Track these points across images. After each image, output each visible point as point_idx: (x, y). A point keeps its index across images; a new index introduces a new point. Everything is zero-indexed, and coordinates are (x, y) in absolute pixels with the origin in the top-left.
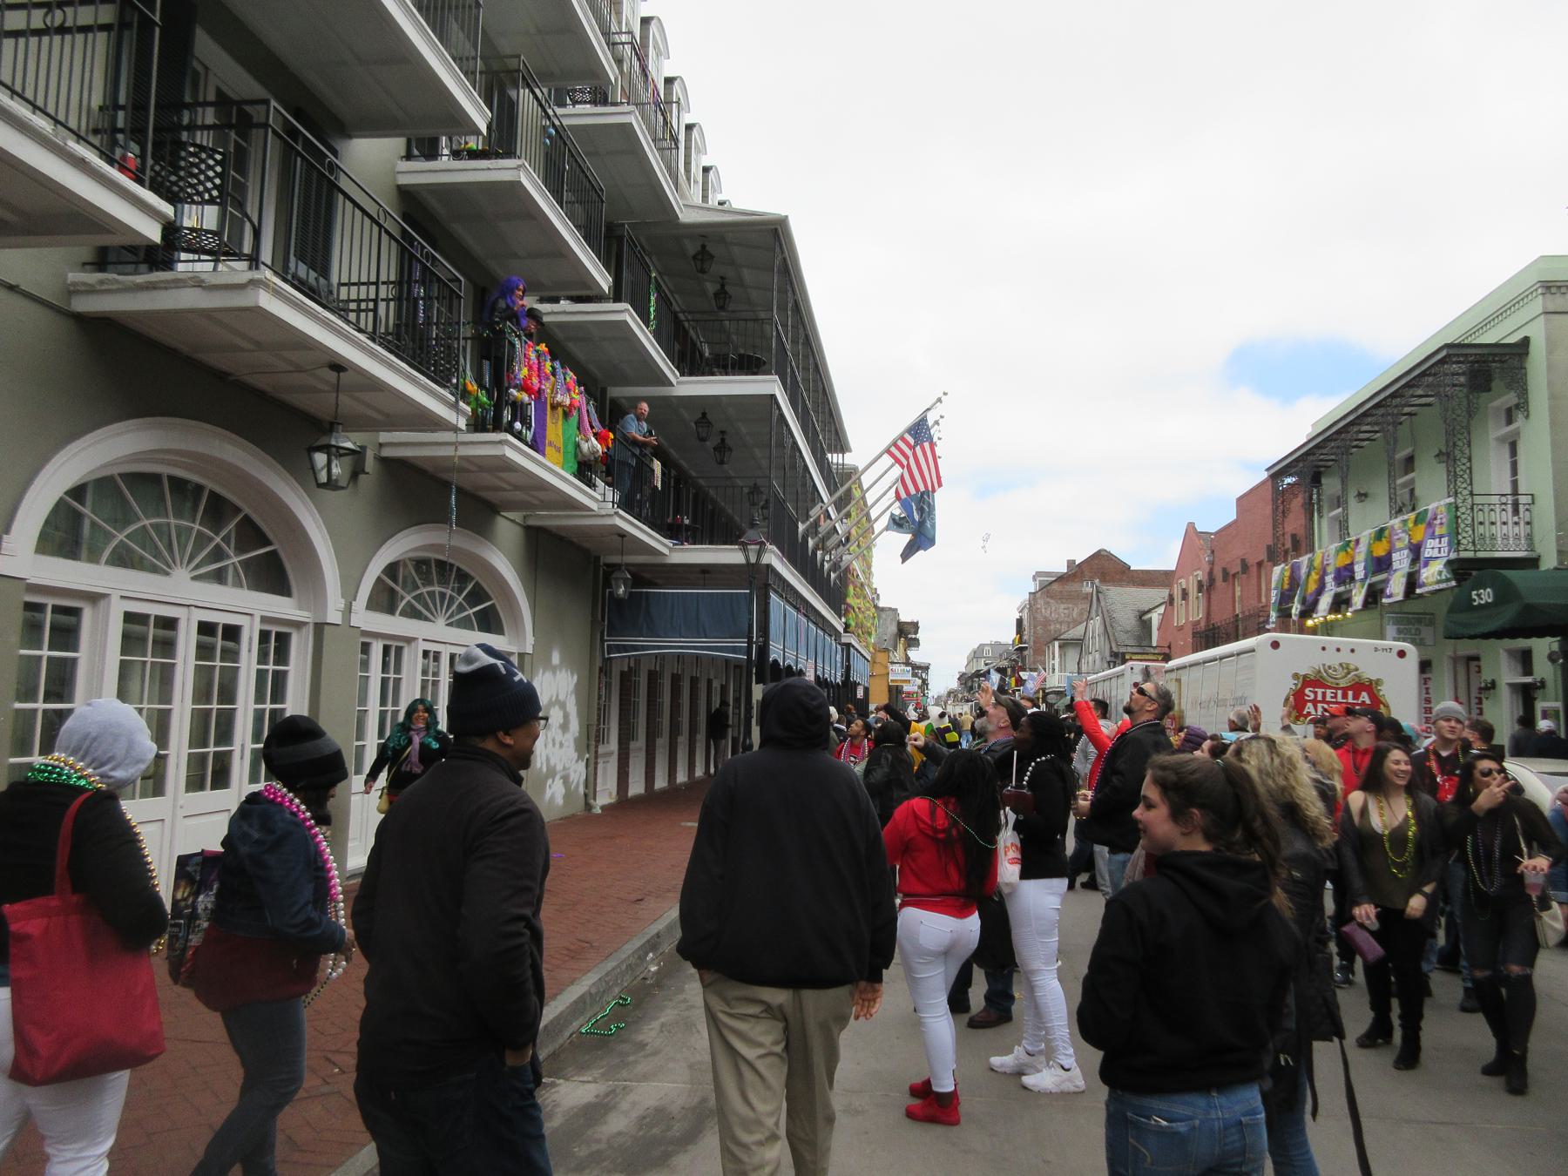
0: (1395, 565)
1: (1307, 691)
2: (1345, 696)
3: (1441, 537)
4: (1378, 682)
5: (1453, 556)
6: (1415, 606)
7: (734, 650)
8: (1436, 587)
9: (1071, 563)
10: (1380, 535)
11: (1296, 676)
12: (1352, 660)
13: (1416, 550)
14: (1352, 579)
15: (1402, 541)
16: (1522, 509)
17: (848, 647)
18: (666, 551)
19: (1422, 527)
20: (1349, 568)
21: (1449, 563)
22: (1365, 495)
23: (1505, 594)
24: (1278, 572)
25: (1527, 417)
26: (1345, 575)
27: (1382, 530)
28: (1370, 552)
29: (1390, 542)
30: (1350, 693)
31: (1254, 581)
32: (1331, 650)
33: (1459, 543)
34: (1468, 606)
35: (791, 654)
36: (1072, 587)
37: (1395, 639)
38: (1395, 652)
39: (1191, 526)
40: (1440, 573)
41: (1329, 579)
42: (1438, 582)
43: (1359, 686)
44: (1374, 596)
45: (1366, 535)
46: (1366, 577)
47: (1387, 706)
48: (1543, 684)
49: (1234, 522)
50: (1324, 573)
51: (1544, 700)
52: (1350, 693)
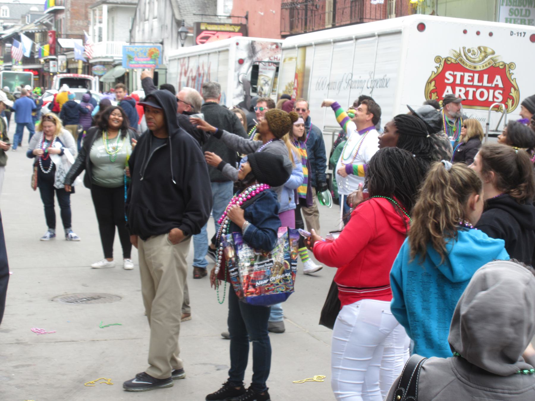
1: (447, 75)
2: (481, 80)
4: (511, 65)
11: (438, 59)
12: (490, 44)
30: (486, 77)
32: (472, 33)
37: (507, 21)
38: (528, 36)
43: (494, 71)
52: (486, 77)
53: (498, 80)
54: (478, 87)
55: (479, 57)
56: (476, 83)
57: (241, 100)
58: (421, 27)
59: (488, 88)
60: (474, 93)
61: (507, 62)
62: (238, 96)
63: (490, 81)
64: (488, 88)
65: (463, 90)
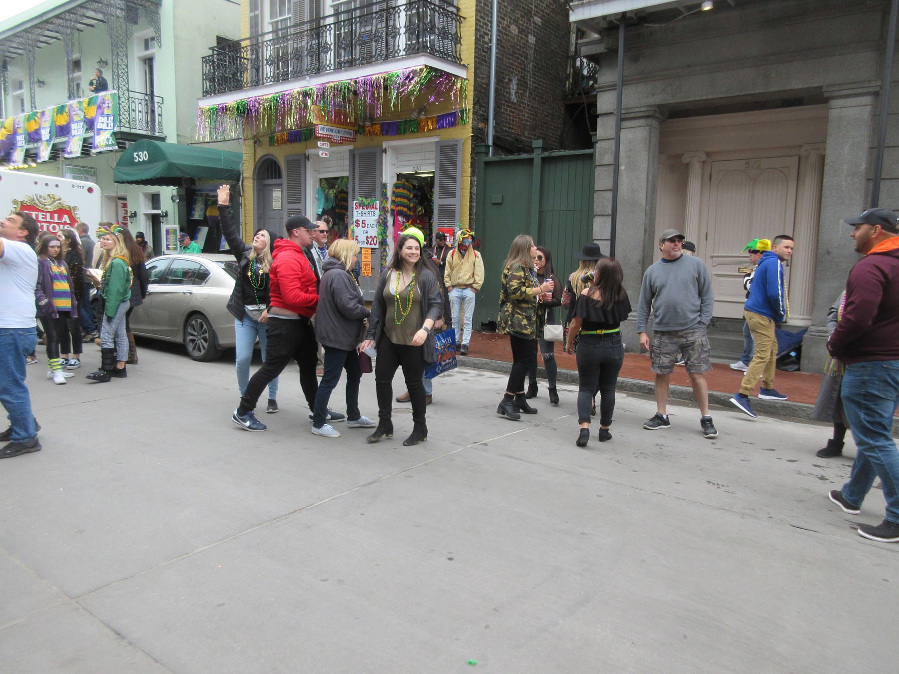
0: (73, 132)
2: (52, 218)
3: (108, 116)
4: (75, 208)
5: (117, 129)
6: (86, 162)
8: (105, 149)
10: (61, 110)
11: (15, 202)
12: (57, 193)
13: (90, 124)
14: (39, 140)
15: (79, 116)
19: (94, 108)
20: (37, 132)
21: (114, 134)
22: (43, 83)
23: (156, 155)
25: (160, 47)
26: (34, 137)
27: (63, 107)
28: (53, 122)
29: (70, 116)
30: (56, 216)
32: (41, 185)
33: (120, 121)
34: (132, 163)
40: (108, 140)
42: (107, 146)
43: (61, 211)
44: (56, 152)
45: (50, 109)
48: (166, 215)
51: (167, 223)
52: (56, 216)
53: (66, 218)
56: (48, 219)
60: (48, 227)
61: (72, 205)
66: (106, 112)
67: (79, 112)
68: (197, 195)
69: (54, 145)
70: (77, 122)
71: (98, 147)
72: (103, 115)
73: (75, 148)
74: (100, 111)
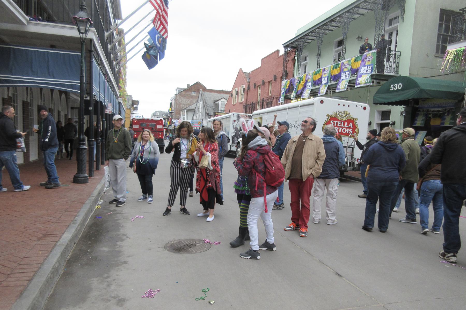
2: (344, 124)
7: (72, 87)
8: (365, 85)
9: (188, 85)
13: (355, 72)
16: (397, 57)
17: (120, 103)
18: (25, 22)
20: (320, 80)
24: (285, 83)
25: (403, 21)
26: (318, 82)
30: (346, 123)
31: (267, 88)
34: (388, 91)
35: (102, 96)
36: (188, 93)
39: (241, 69)
40: (367, 79)
41: (308, 85)
42: (366, 83)
46: (327, 82)
47: (358, 129)
49: (260, 67)
50: (307, 82)
52: (346, 123)
54: (343, 127)
55: (344, 115)
56: (342, 126)
57: (234, 134)
58: (322, 102)
59: (347, 128)
60: (341, 129)
62: (233, 133)
63: (348, 125)
64: (347, 128)
65: (337, 128)
66: (367, 64)
67: (348, 66)
68: (419, 111)
69: (329, 86)
70: (345, 72)
71: (359, 84)
72: (364, 65)
73: (343, 86)
74: (363, 63)
